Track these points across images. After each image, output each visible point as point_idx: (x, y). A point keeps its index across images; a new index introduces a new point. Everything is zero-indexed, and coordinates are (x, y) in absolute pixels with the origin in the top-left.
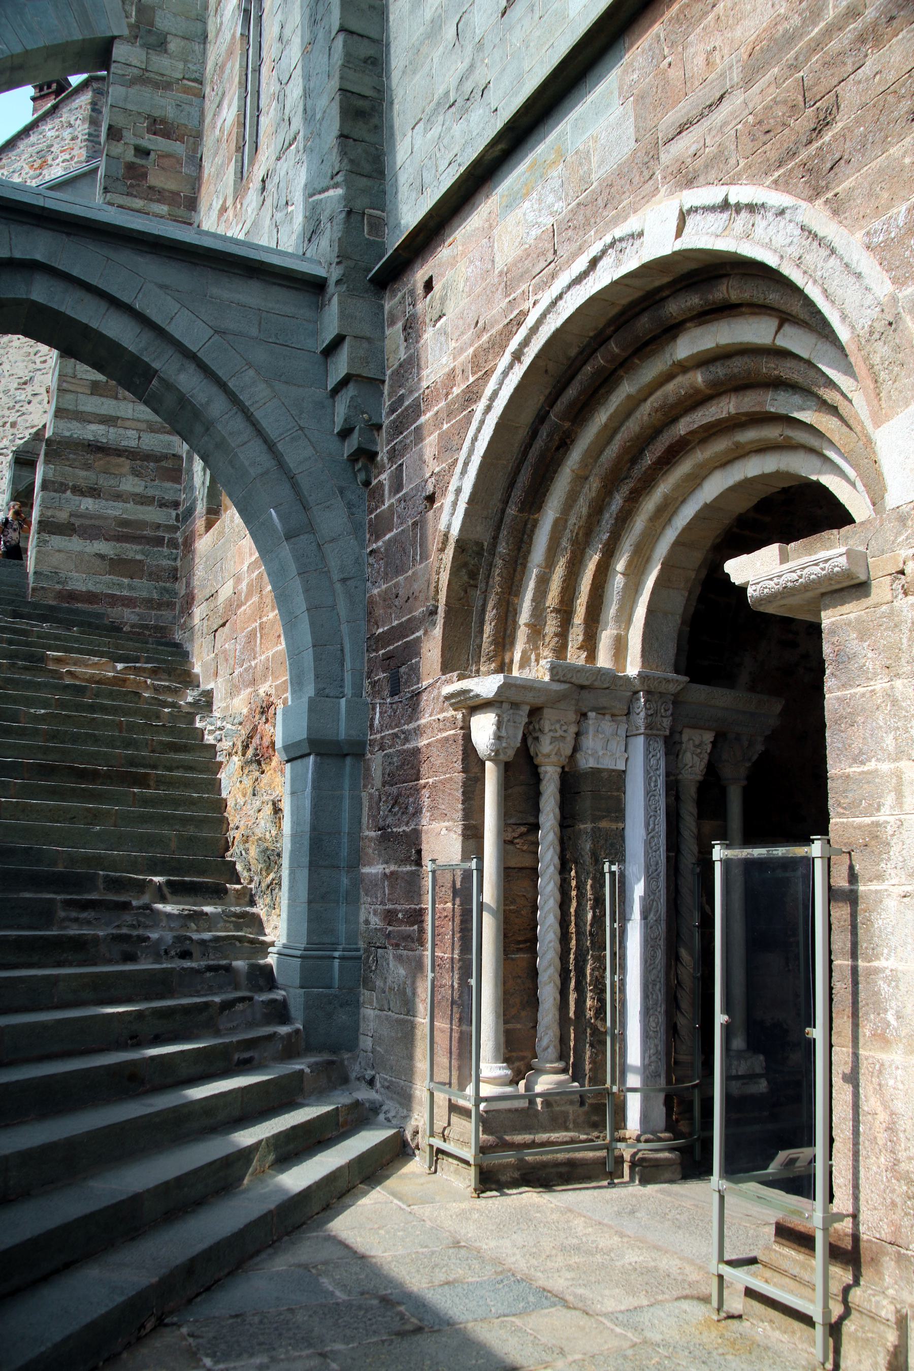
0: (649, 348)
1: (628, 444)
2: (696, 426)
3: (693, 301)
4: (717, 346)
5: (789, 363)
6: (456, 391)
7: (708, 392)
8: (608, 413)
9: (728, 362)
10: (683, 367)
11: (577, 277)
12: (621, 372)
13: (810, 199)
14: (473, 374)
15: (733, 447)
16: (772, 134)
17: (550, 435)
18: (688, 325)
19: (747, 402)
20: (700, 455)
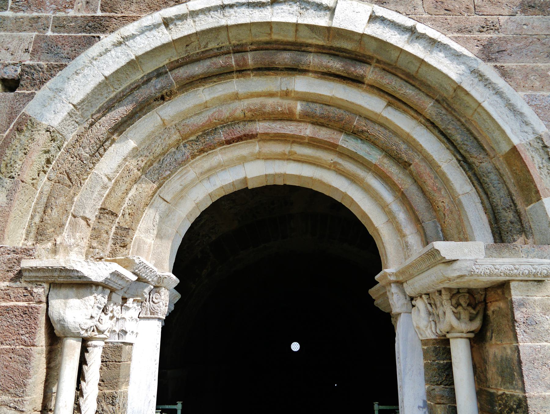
0: (267, 73)
1: (214, 121)
2: (273, 132)
3: (336, 65)
4: (331, 98)
5: (377, 127)
6: (72, 13)
7: (298, 118)
8: (212, 96)
9: (327, 108)
10: (286, 94)
11: (254, 3)
12: (235, 75)
13: (484, 61)
14: (103, 10)
15: (287, 153)
16: (450, 13)
17: (162, 88)
18: (310, 74)
19: (323, 134)
20: (255, 147)
